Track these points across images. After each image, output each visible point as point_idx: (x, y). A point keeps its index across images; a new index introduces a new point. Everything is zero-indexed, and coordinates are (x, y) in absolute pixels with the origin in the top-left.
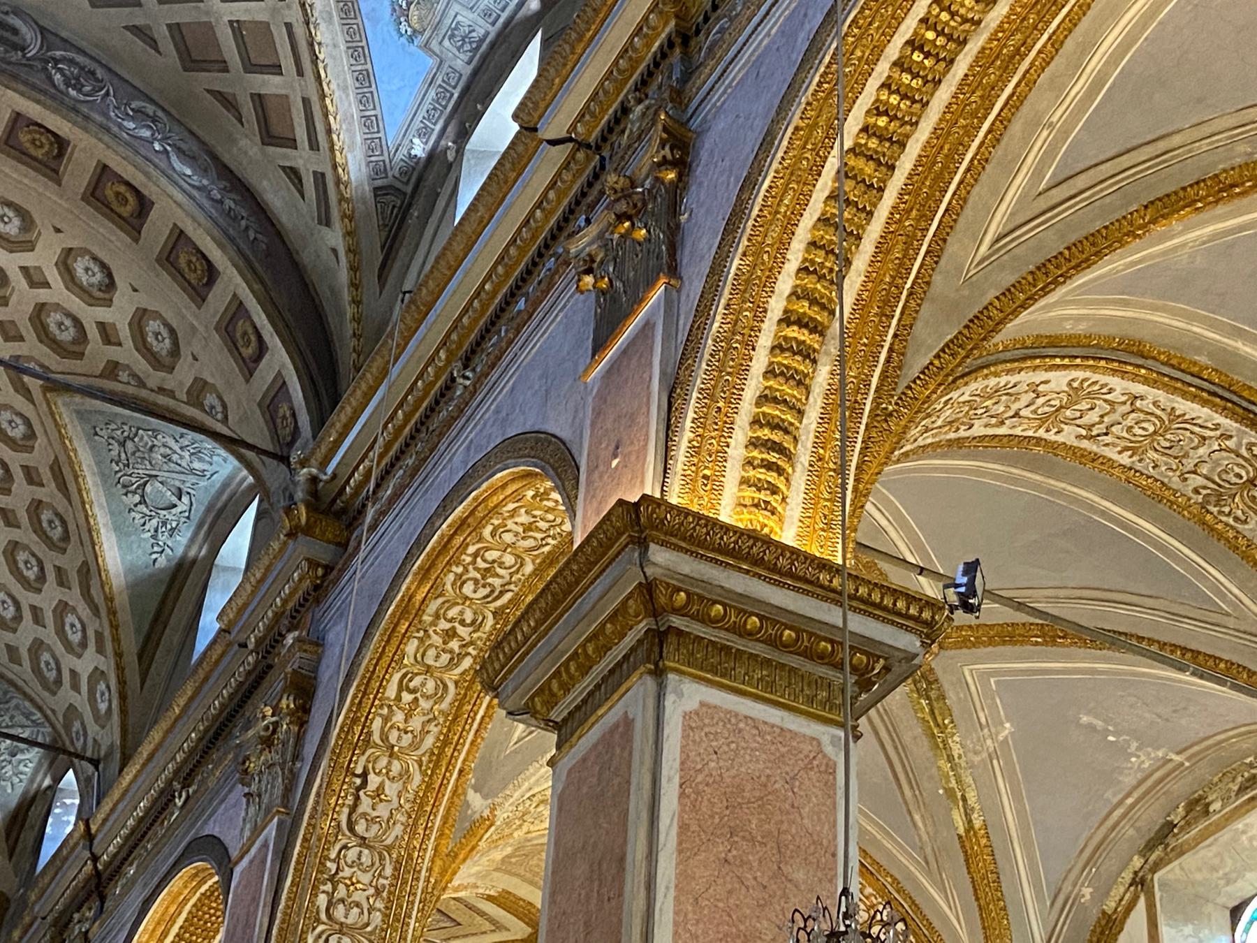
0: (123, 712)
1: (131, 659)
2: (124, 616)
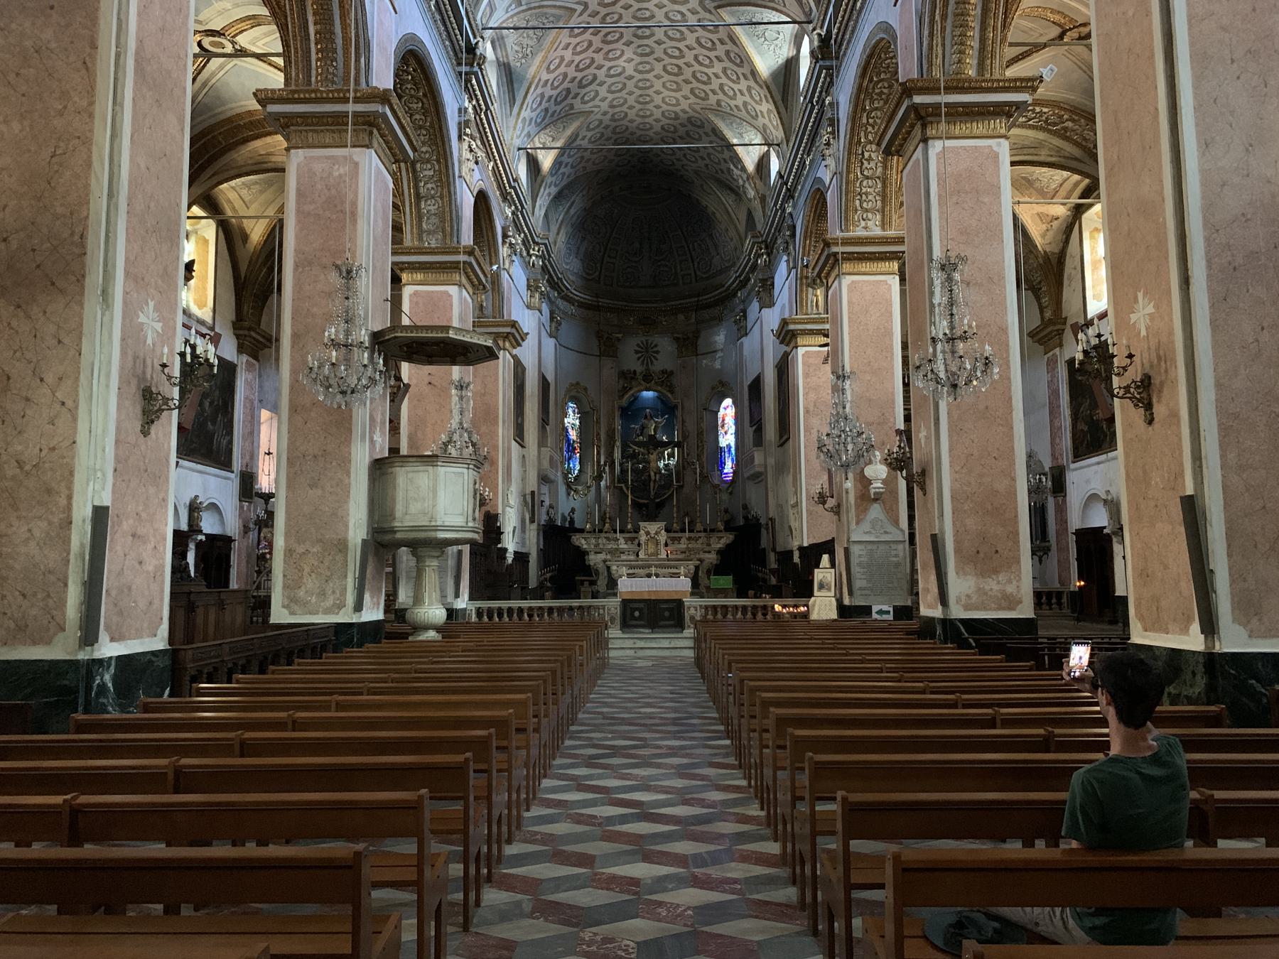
0: (782, 124)
1: (780, 103)
2: (773, 88)
